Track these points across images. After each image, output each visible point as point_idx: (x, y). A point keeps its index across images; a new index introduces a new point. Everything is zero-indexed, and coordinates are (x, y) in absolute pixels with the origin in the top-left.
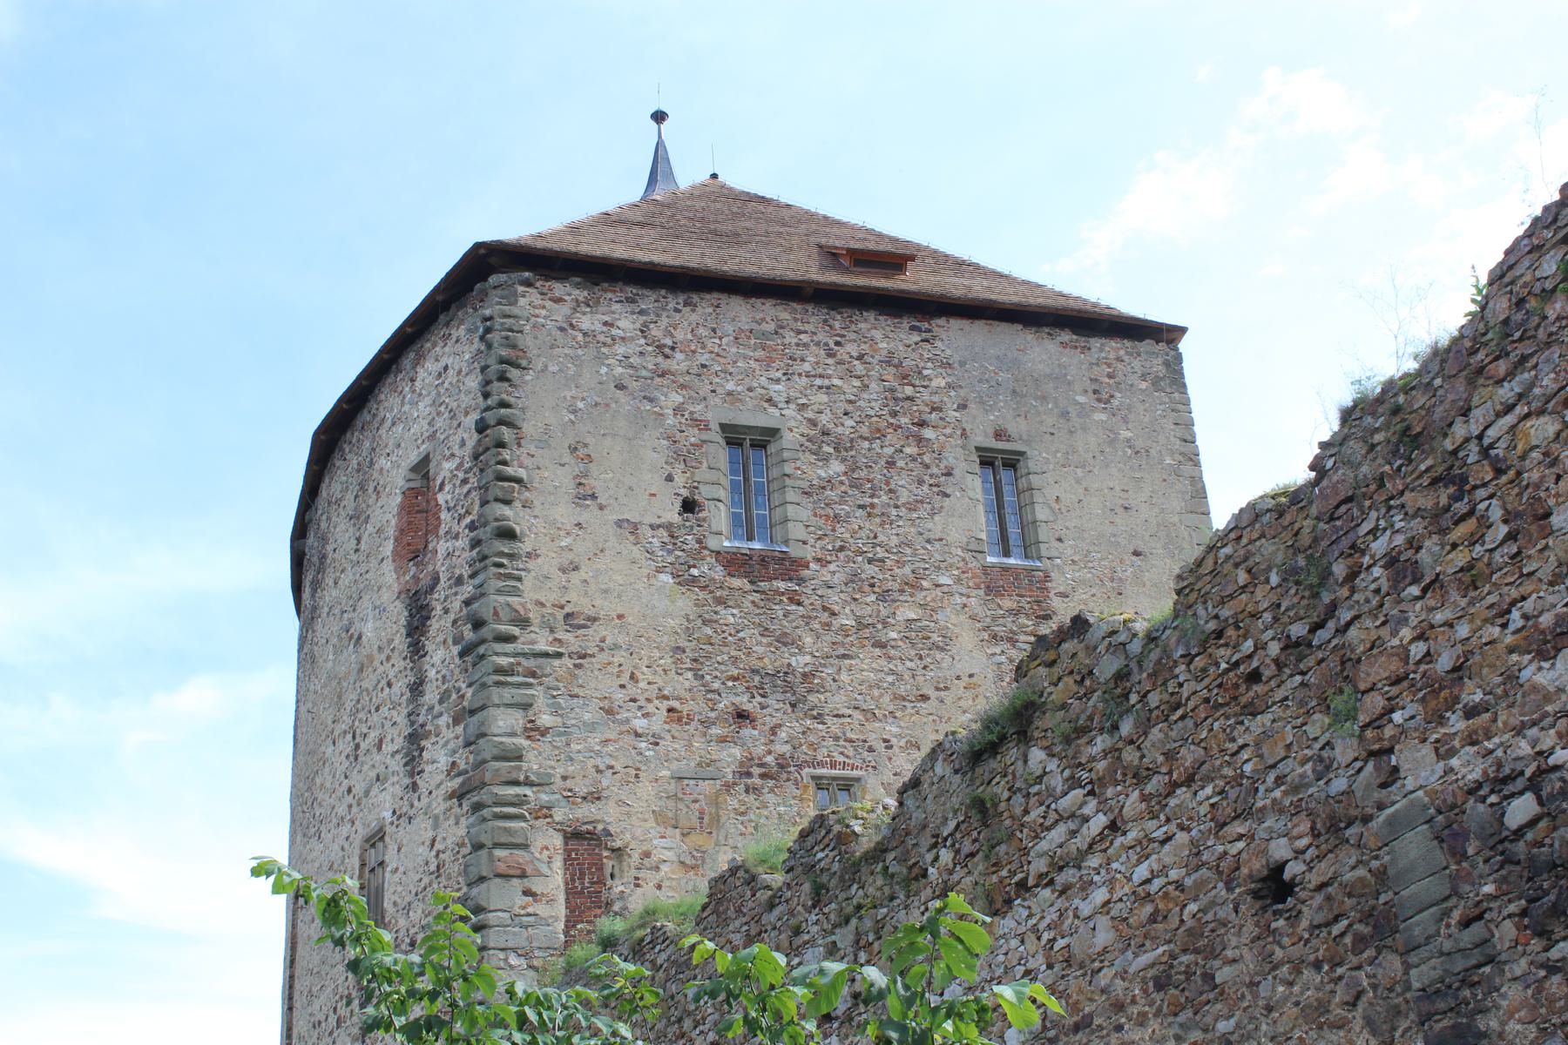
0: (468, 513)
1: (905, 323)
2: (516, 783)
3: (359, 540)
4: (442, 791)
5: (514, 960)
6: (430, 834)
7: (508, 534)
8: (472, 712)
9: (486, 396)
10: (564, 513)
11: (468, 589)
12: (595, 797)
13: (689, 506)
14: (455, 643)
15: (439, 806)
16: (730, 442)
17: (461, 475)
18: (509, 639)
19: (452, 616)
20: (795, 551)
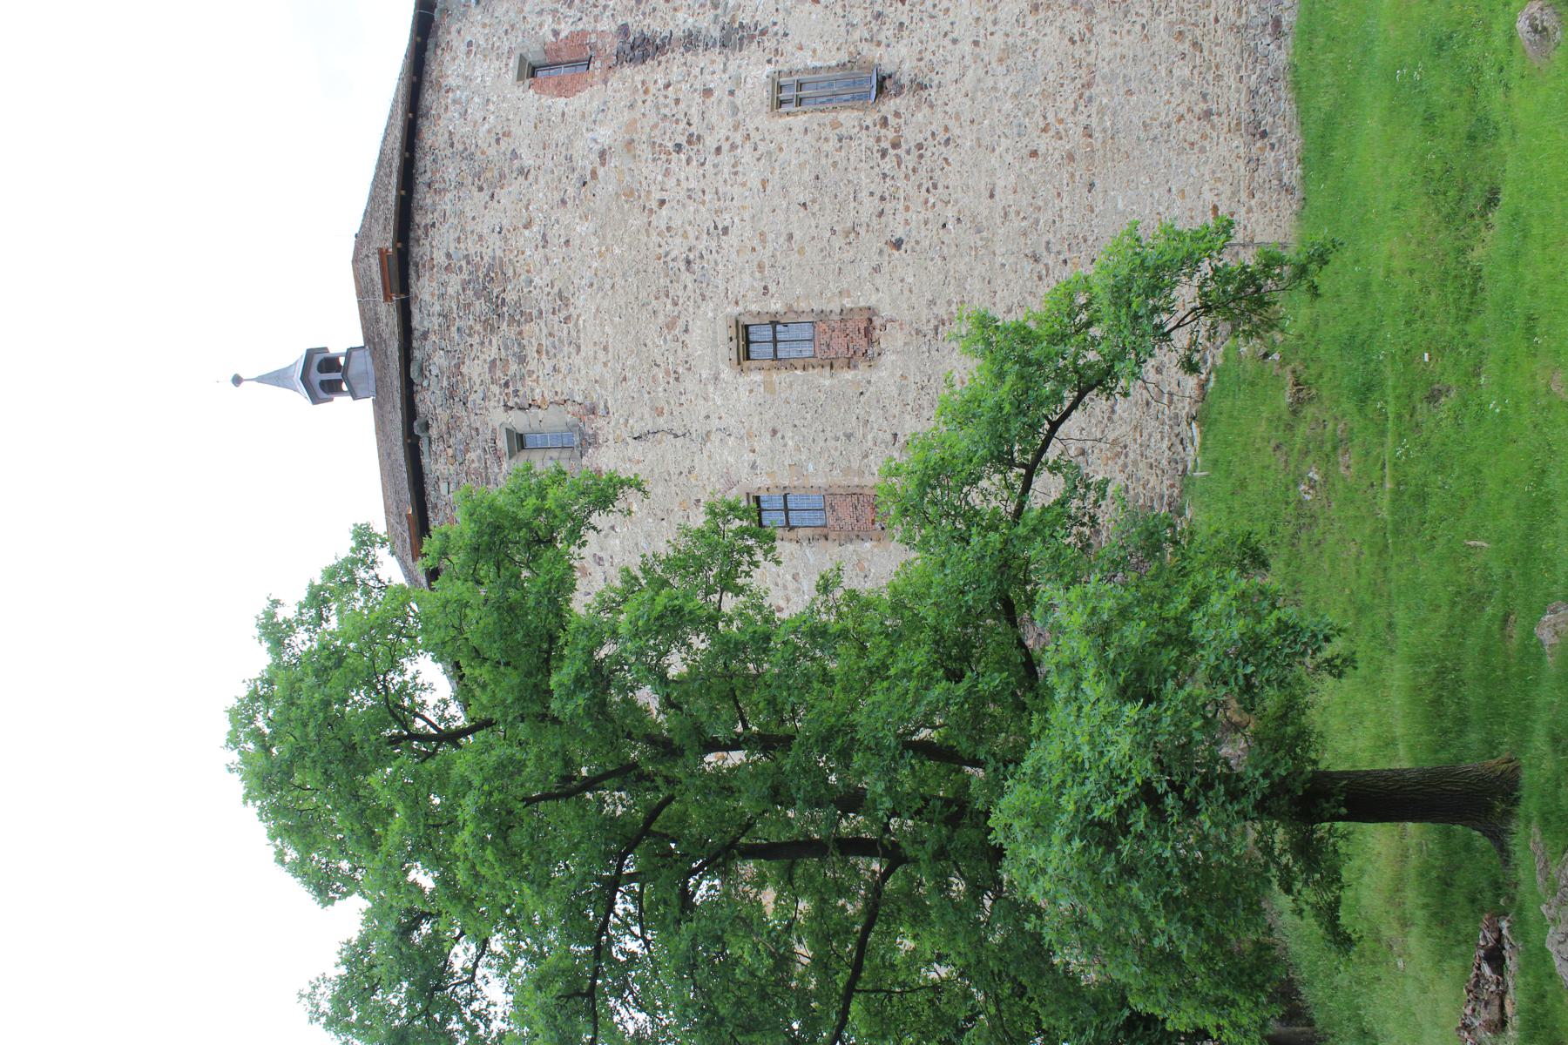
3: (524, 172)
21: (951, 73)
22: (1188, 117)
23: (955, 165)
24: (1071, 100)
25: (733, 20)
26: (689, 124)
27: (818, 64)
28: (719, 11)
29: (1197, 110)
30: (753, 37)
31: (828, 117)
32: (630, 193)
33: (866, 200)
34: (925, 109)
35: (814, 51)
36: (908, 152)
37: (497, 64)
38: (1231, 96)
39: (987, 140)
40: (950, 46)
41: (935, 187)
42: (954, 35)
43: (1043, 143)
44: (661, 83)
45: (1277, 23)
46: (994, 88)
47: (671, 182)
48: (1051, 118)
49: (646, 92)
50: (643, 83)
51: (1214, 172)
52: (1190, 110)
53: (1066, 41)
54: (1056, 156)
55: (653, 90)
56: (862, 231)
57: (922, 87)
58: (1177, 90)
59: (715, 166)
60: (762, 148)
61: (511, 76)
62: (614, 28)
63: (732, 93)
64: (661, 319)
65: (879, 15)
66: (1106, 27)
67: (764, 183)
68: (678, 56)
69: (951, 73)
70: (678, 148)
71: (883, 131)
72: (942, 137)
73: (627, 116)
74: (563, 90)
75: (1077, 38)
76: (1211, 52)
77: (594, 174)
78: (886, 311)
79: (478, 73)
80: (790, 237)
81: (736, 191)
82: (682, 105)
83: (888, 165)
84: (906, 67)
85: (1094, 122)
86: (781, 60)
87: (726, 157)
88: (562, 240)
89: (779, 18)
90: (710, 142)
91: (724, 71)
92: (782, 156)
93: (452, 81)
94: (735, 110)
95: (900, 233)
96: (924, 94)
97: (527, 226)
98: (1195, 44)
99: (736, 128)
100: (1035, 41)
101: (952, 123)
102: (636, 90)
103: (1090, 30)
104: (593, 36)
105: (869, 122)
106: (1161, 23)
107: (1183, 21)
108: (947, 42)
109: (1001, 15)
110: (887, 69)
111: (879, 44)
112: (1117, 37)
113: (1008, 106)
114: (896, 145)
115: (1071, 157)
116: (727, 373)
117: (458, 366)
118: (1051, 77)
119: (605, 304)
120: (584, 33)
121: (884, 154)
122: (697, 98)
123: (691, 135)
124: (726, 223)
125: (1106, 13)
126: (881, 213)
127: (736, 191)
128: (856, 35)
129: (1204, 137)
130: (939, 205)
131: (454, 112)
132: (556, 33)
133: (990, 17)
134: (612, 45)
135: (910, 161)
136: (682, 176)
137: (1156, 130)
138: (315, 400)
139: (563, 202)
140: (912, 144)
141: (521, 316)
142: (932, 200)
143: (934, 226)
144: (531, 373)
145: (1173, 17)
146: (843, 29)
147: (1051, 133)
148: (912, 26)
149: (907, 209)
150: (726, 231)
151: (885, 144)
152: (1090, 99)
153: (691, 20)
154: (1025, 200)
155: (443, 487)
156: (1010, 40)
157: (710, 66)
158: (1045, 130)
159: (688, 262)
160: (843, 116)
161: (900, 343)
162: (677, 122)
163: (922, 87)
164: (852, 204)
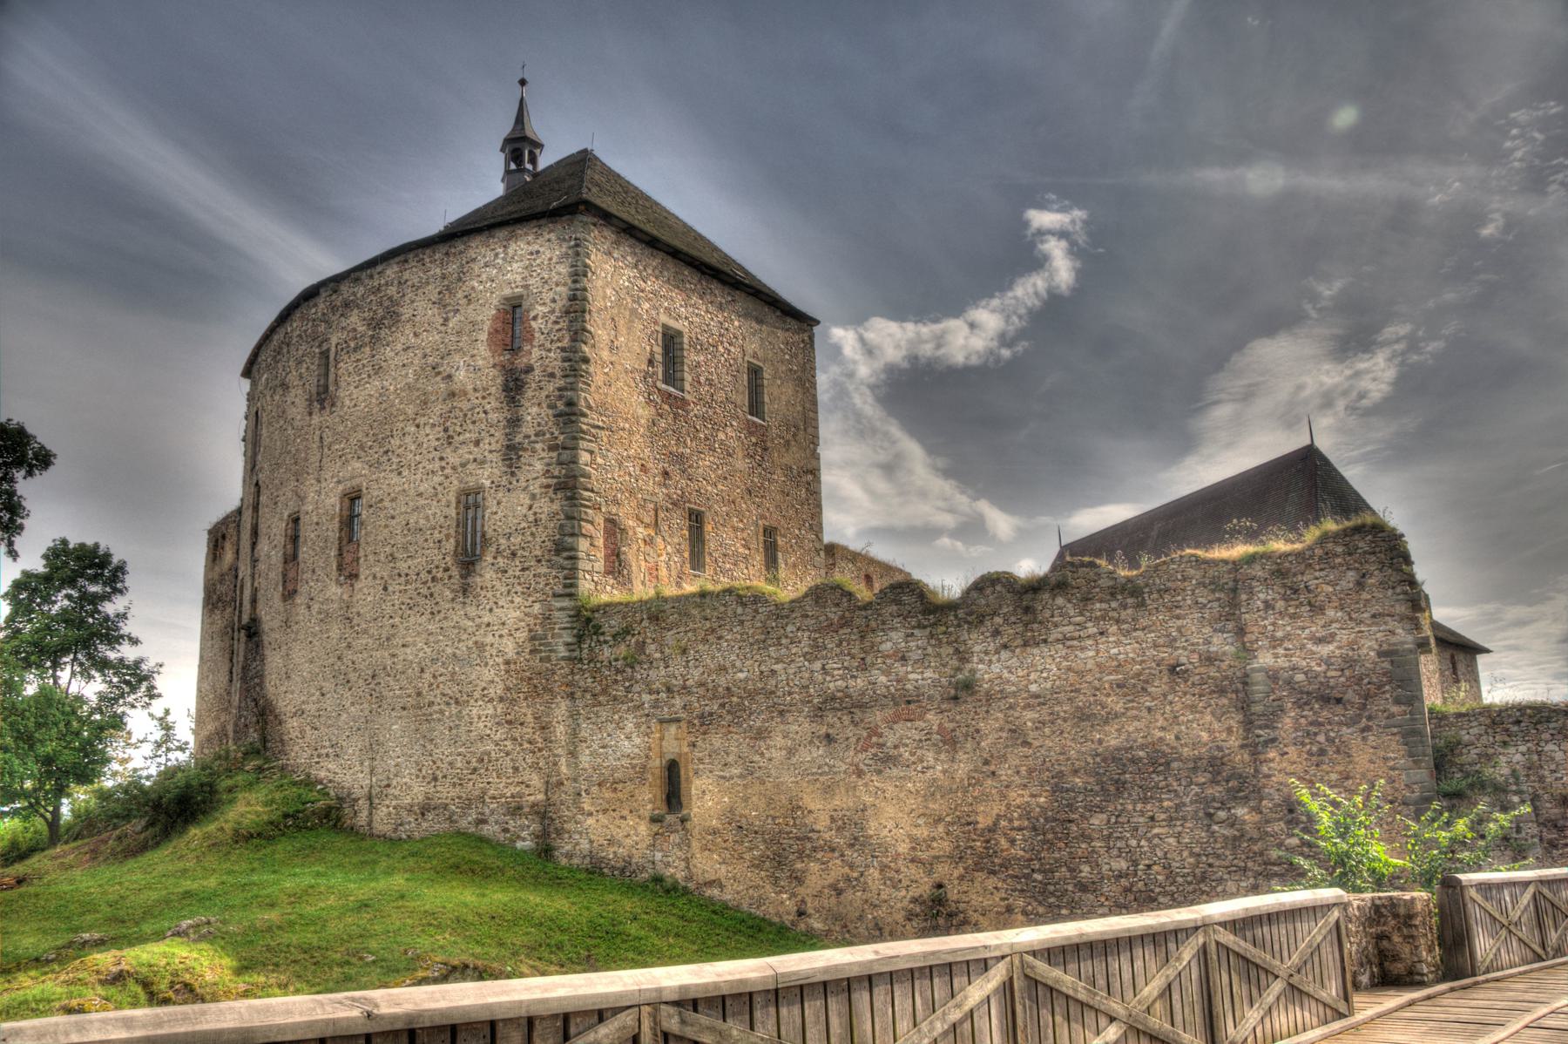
0: (559, 340)
1: (727, 290)
3: (446, 320)
4: (538, 483)
6: (528, 502)
7: (586, 360)
9: (575, 282)
10: (605, 354)
11: (561, 383)
12: (616, 502)
13: (651, 362)
14: (550, 407)
15: (535, 488)
16: (664, 335)
17: (553, 318)
18: (585, 415)
19: (544, 393)
20: (687, 397)
30: (510, 466)
31: (452, 531)
34: (451, 596)
37: (519, 278)
38: (445, 792)
39: (431, 639)
43: (427, 676)
45: (484, 822)
48: (441, 679)
57: (465, 591)
60: (440, 488)
61: (507, 292)
65: (514, 554)
66: (491, 711)
67: (420, 495)
69: (472, 611)
70: (446, 430)
72: (436, 609)
73: (470, 387)
74: (494, 333)
77: (439, 373)
78: (358, 585)
79: (515, 265)
81: (418, 476)
83: (424, 575)
84: (478, 579)
85: (436, 708)
87: (437, 464)
93: (513, 247)
95: (390, 589)
97: (416, 335)
98: (475, 769)
99: (454, 468)
102: (485, 389)
106: (490, 747)
110: (478, 567)
113: (449, 651)
115: (419, 694)
116: (341, 487)
117: (358, 306)
120: (531, 339)
122: (474, 436)
127: (418, 476)
128: (503, 541)
131: (490, 256)
132: (535, 318)
134: (521, 362)
135: (424, 591)
137: (429, 747)
138: (502, 150)
139: (425, 356)
141: (375, 340)
143: (388, 610)
152: (448, 704)
158: (434, 677)
160: (452, 540)
161: (345, 597)
163: (465, 591)
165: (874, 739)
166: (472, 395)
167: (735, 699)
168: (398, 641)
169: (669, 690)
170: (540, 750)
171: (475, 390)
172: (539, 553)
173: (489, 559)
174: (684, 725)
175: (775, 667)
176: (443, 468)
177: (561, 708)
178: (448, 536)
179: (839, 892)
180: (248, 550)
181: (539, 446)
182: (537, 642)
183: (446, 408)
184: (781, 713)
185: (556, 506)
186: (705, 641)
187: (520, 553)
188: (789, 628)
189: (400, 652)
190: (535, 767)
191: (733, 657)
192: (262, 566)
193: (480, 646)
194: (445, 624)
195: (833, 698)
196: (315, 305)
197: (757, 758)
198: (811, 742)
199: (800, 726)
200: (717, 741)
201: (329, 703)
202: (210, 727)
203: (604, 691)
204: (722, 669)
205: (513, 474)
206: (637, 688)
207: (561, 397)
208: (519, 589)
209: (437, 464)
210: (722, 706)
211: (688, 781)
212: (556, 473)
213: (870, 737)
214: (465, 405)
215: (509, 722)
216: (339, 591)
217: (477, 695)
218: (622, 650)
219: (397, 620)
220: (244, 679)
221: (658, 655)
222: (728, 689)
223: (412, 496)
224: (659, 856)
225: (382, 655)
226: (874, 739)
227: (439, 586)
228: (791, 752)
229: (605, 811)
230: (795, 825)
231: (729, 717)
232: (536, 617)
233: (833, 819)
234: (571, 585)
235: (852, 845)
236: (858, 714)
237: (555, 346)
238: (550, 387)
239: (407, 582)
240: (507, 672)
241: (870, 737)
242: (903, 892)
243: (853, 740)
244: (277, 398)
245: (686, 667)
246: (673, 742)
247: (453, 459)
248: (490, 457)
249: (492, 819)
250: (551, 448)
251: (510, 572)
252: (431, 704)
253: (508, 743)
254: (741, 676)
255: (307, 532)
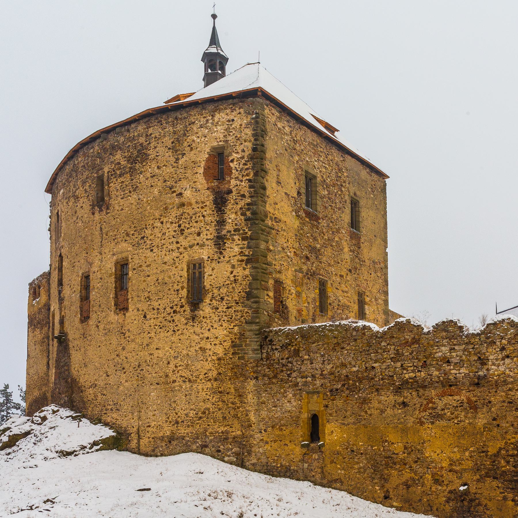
2: (265, 264)
5: (265, 313)
6: (231, 270)
8: (252, 239)
11: (249, 200)
14: (242, 214)
15: (234, 261)
21: (198, 330)
22: (177, 416)
23: (166, 335)
24: (185, 375)
25: (228, 239)
26: (188, 228)
27: (205, 278)
28: (233, 232)
29: (179, 419)
31: (185, 285)
32: (166, 209)
33: (157, 304)
34: (185, 322)
35: (211, 275)
36: (172, 317)
40: (207, 328)
41: (161, 328)
42: (211, 329)
43: (172, 366)
44: (205, 213)
46: (191, 347)
47: (168, 225)
48: (179, 368)
49: (202, 208)
50: (206, 206)
51: (160, 425)
52: (179, 417)
53: (206, 371)
54: (168, 371)
55: (203, 210)
56: (149, 303)
58: (185, 412)
59: (172, 242)
62: (231, 187)
63: (198, 244)
64: (129, 230)
65: (222, 299)
67: (165, 263)
68: (215, 218)
69: (198, 330)
70: (180, 226)
71: (179, 306)
72: (176, 329)
75: (207, 375)
76: (197, 423)
80: (149, 276)
81: (164, 252)
82: (195, 224)
83: (168, 310)
84: (201, 312)
86: (209, 262)
87: (175, 246)
88: (153, 184)
89: (227, 259)
90: (181, 239)
91: (207, 239)
92: (174, 268)
94: (191, 247)
95: (148, 317)
96: (191, 321)
98: (201, 418)
99: (185, 248)
100: (207, 360)
101: (180, 332)
102: (203, 202)
103: (208, 381)
104: (229, 179)
105: (183, 300)
106: (209, 405)
107: (209, 414)
108: (209, 327)
109: (217, 347)
110: (201, 306)
111: (211, 301)
112: (205, 390)
113: (185, 352)
114: (175, 312)
115: (167, 376)
118: (193, 367)
119: (134, 207)
121: (172, 308)
122: (197, 230)
123: (184, 231)
124: (154, 251)
125: (215, 385)
126: (154, 309)
127: (164, 252)
128: (215, 291)
129: (170, 422)
130: (155, 330)
133: (217, 342)
135: (169, 318)
136: (170, 230)
137: (173, 405)
140: (174, 318)
141: (132, 171)
142: (156, 327)
143: (147, 329)
144: (117, 180)
145: (211, 410)
146: (219, 285)
147: (175, 369)
148: (216, 312)
149: (154, 319)
150: (152, 250)
151: (175, 307)
152: (184, 381)
153: (230, 221)
154: (155, 361)
155: (92, 151)
156: (207, 351)
157: (209, 233)
158: (176, 367)
159: (143, 238)
160: (185, 290)
162: (189, 223)
163: (193, 319)
164: (157, 298)
165: (430, 405)
166: (195, 206)
167: (351, 382)
168: (153, 346)
169: (313, 376)
170: (238, 408)
171: (197, 202)
172: (238, 299)
173: (207, 301)
174: (321, 395)
175: (375, 365)
176: (178, 248)
177: (251, 385)
178: (183, 288)
179: (408, 487)
180: (57, 293)
181: (236, 237)
182: (237, 346)
183: (179, 213)
184: (377, 390)
185: (247, 272)
186: (334, 349)
187: (226, 298)
188: (383, 344)
189: (156, 353)
190: (236, 416)
191: (350, 359)
192: (66, 303)
193: (203, 350)
194: (181, 337)
195: (407, 382)
196: (93, 147)
197: (363, 414)
198: (394, 406)
199: (388, 397)
200: (339, 403)
201: (112, 380)
202: (36, 393)
203: (275, 377)
204: (344, 365)
205: (221, 253)
206: (294, 375)
207: (248, 209)
208: (226, 318)
209: (175, 246)
210: (343, 385)
211: (324, 425)
212: (247, 253)
213: (428, 404)
214: (191, 212)
215: (220, 392)
216: (116, 317)
217: (201, 377)
218: (286, 354)
219: (153, 334)
220: (57, 367)
221: (306, 357)
222: (347, 376)
223: (161, 266)
224: (306, 465)
225: (144, 354)
226: (430, 405)
227: (178, 315)
228: (382, 411)
229: (275, 441)
230: (384, 450)
231: (347, 392)
232: (236, 334)
233: (405, 448)
234: (257, 317)
235: (416, 462)
236: (421, 391)
237: (244, 179)
238: (242, 203)
239: (158, 313)
240: (219, 364)
241: (428, 404)
242: (445, 488)
243: (418, 406)
244: (70, 204)
245: (323, 363)
246: (316, 405)
247: (185, 243)
248: (207, 243)
249: (210, 445)
250: (243, 239)
251: (220, 309)
252: (174, 381)
253: (220, 403)
254: (355, 369)
255: (94, 283)
